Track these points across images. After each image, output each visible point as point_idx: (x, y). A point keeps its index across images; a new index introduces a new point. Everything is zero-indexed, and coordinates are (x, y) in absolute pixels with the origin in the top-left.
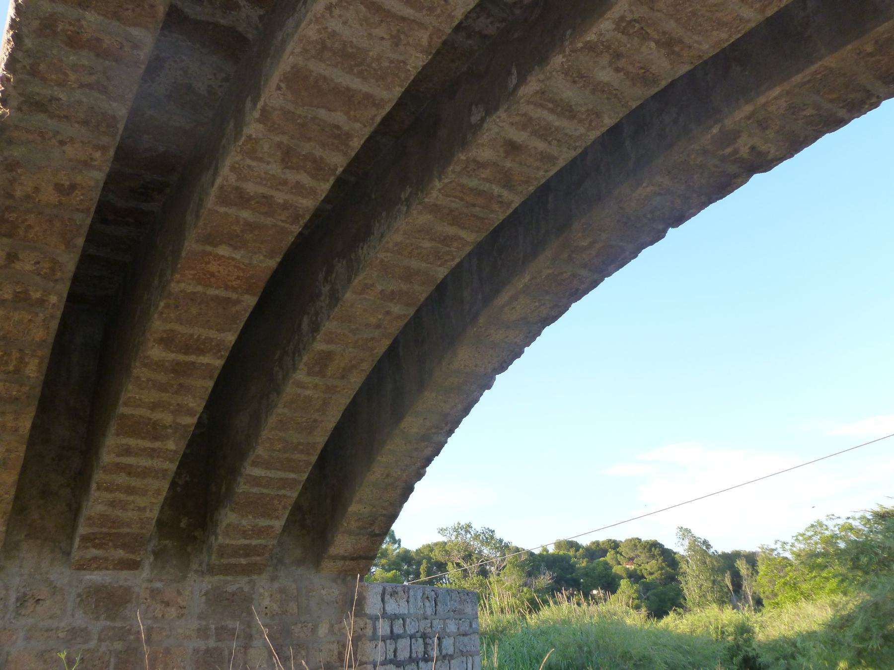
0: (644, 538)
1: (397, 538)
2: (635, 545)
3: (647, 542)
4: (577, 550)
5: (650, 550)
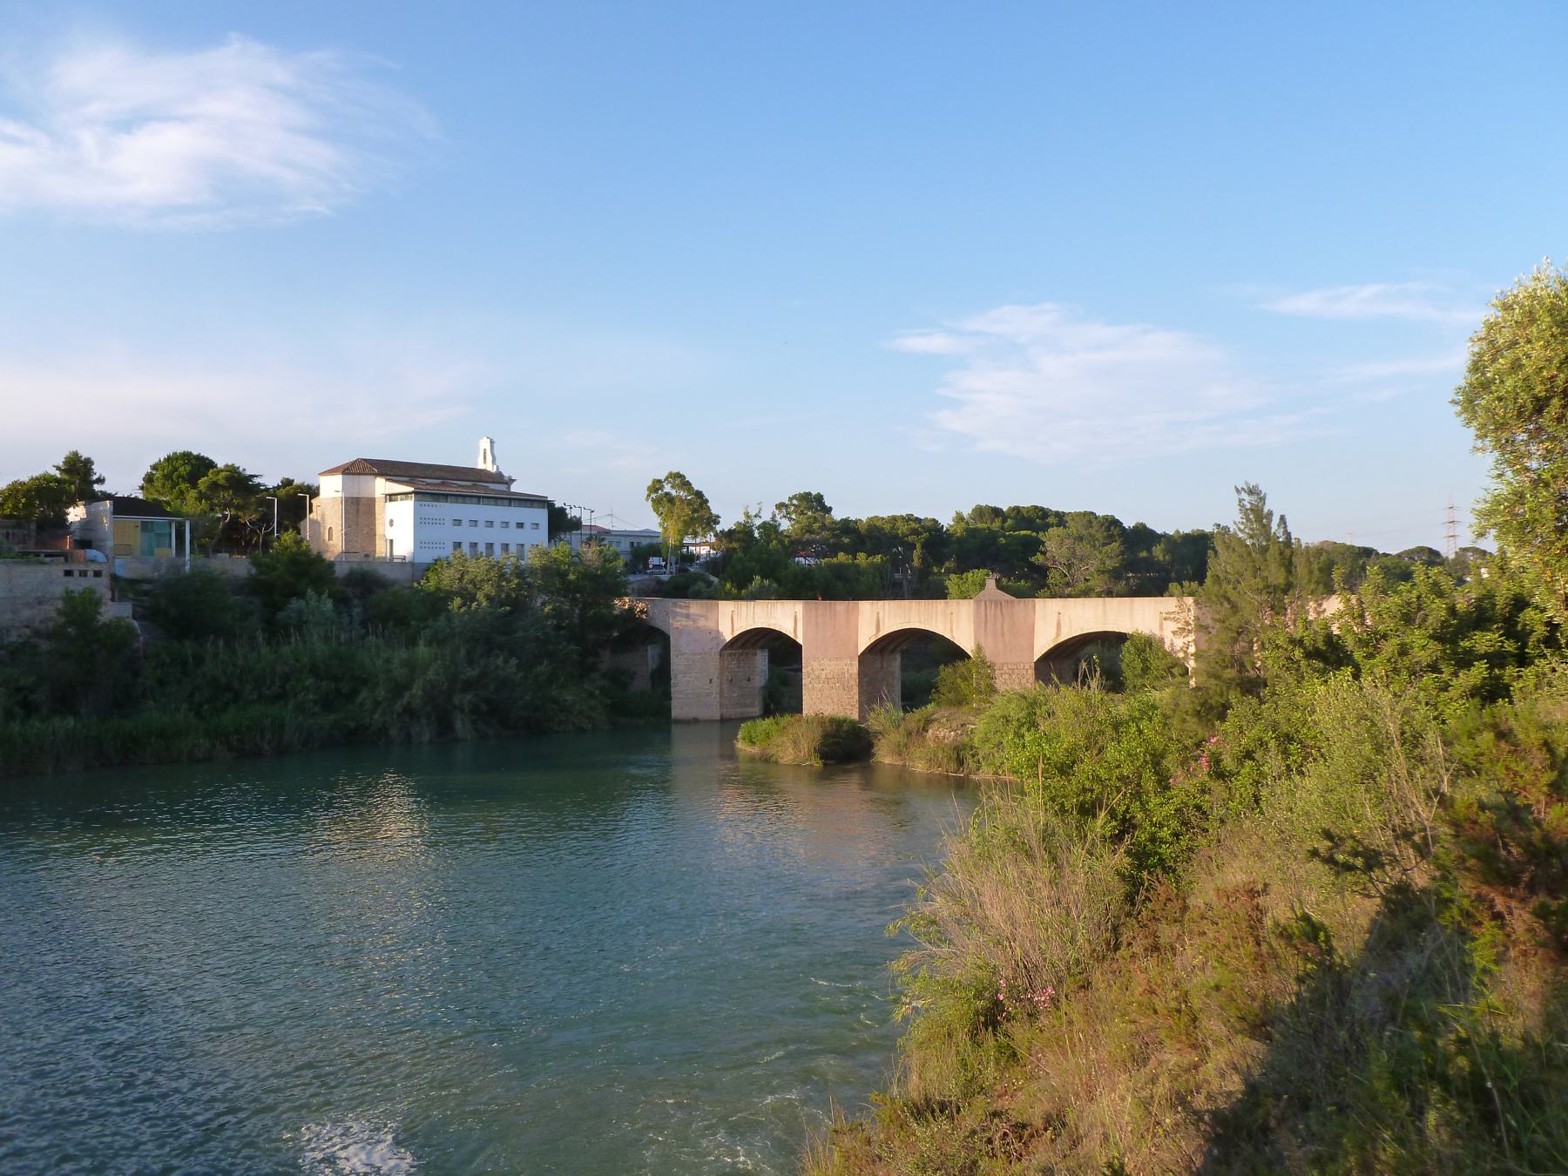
0: (1100, 513)
1: (828, 504)
2: (1090, 522)
3: (1106, 518)
4: (1004, 521)
5: (1108, 529)
